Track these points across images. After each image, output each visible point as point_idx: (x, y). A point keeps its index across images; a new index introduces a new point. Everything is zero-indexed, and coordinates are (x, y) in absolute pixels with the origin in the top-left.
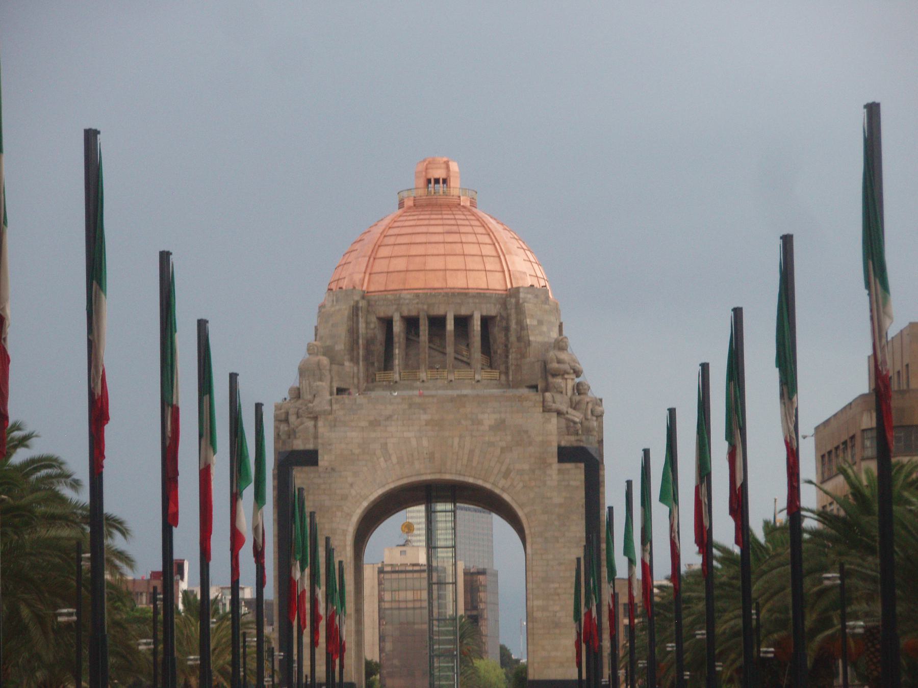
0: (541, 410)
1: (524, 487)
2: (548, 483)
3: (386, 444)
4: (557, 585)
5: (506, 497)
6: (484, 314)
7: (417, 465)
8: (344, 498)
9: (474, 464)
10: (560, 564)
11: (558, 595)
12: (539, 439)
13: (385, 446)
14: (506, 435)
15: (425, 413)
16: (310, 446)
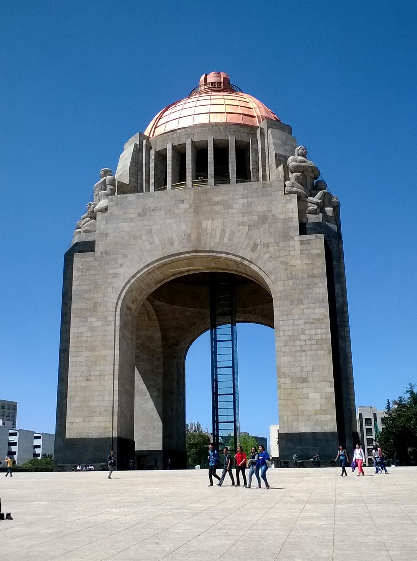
0: (284, 194)
1: (270, 257)
2: (292, 252)
3: (151, 230)
4: (303, 343)
5: (253, 266)
6: (239, 139)
7: (176, 243)
9: (226, 241)
10: (306, 323)
11: (305, 351)
12: (282, 216)
13: (150, 232)
14: (253, 215)
15: (183, 203)
16: (90, 238)
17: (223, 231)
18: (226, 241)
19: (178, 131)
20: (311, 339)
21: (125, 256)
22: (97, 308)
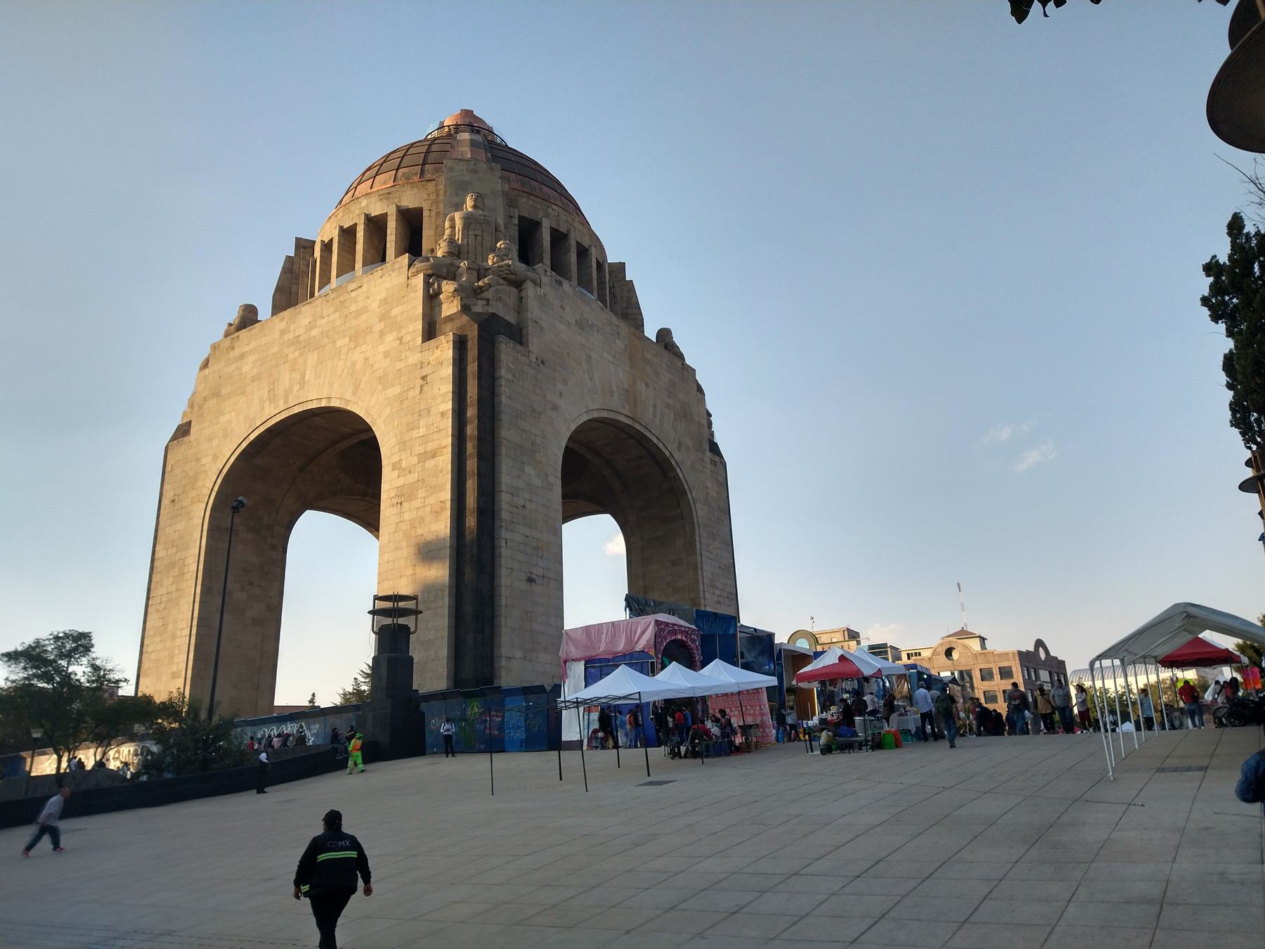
5: (678, 470)
8: (555, 408)
10: (720, 567)
13: (589, 358)
15: (619, 339)
17: (655, 406)
18: (657, 422)
19: (554, 207)
20: (723, 590)
21: (565, 382)
22: (535, 452)
